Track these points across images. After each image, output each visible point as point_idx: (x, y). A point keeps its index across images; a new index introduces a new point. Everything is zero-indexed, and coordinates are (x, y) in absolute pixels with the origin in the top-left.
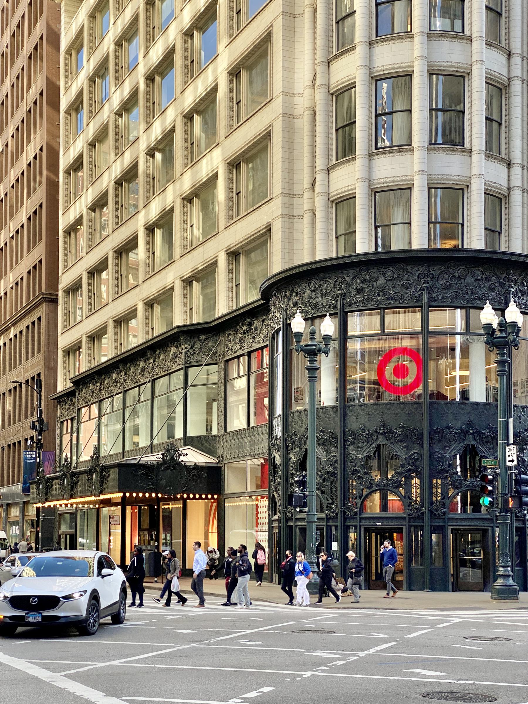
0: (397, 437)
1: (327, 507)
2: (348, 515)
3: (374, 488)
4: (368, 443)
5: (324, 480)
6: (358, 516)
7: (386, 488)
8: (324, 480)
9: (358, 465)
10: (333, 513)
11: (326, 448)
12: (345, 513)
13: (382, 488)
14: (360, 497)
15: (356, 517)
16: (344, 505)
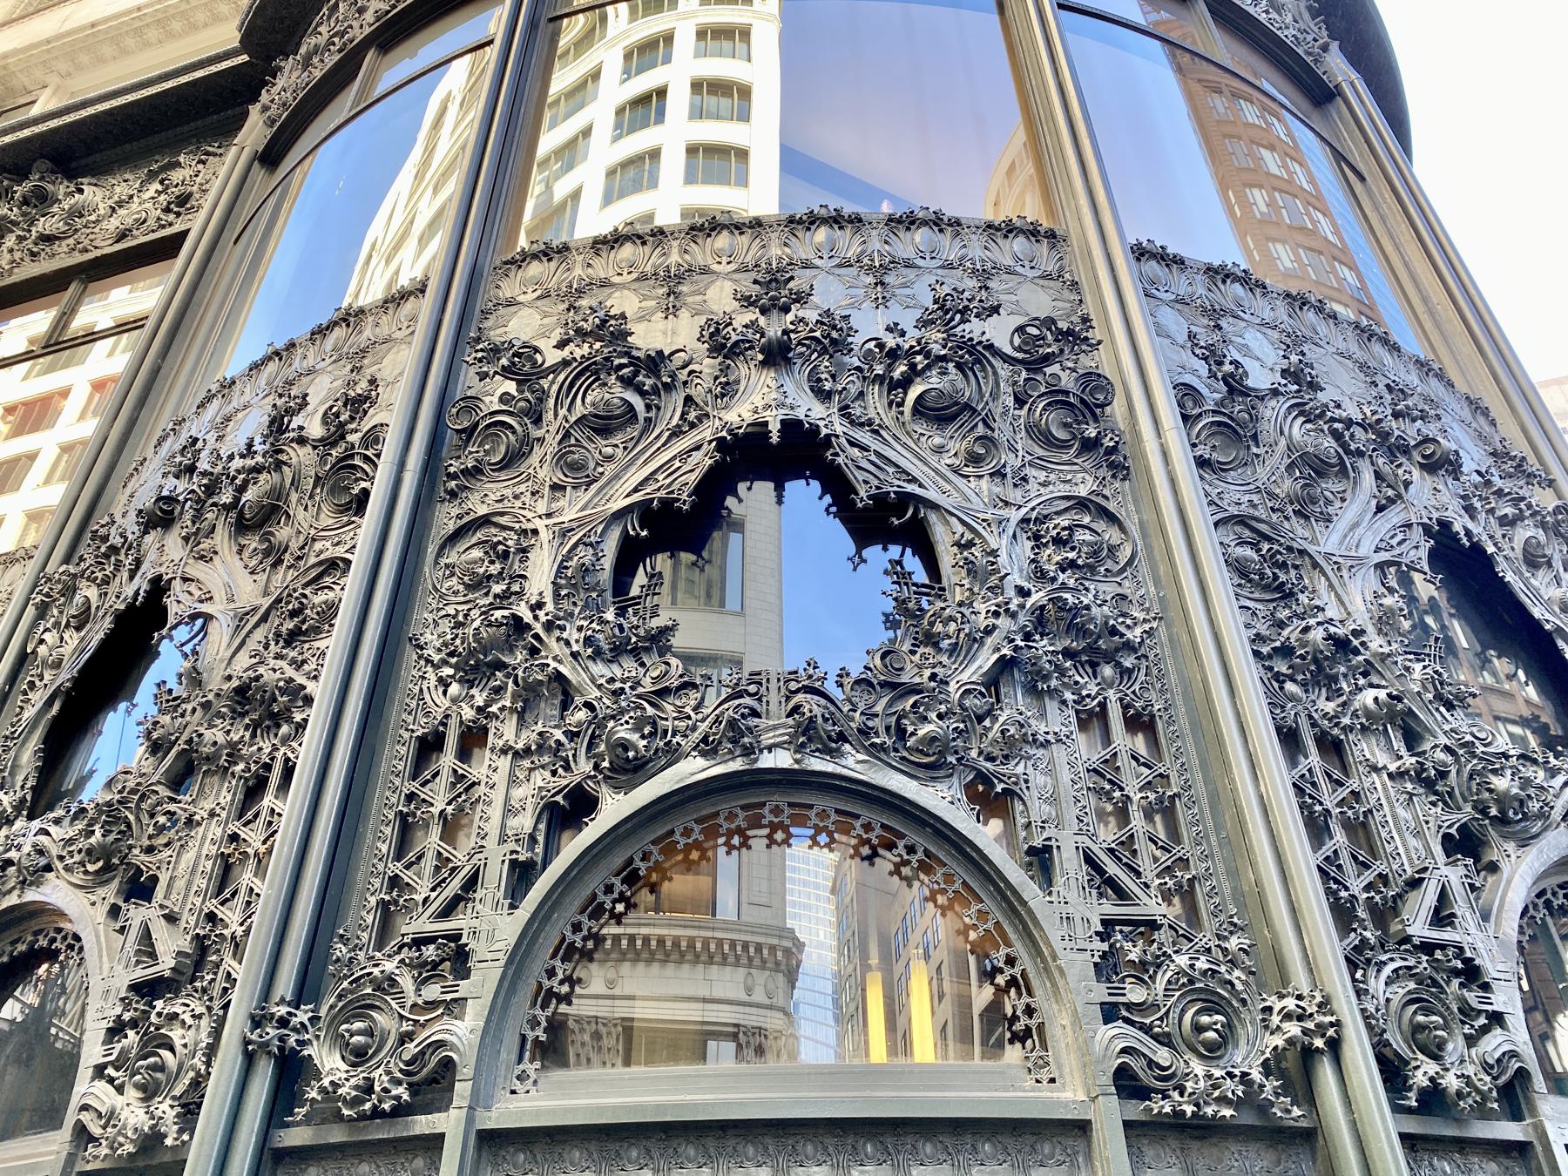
0: (906, 383)
1: (116, 1031)
2: (328, 1112)
3: (693, 769)
4: (645, 431)
5: (178, 780)
6: (448, 1123)
7: (817, 764)
8: (178, 780)
9: (540, 574)
10: (149, 1092)
11: (282, 533)
12: (292, 1070)
13: (782, 759)
14: (522, 874)
15: (423, 1124)
16: (306, 991)
